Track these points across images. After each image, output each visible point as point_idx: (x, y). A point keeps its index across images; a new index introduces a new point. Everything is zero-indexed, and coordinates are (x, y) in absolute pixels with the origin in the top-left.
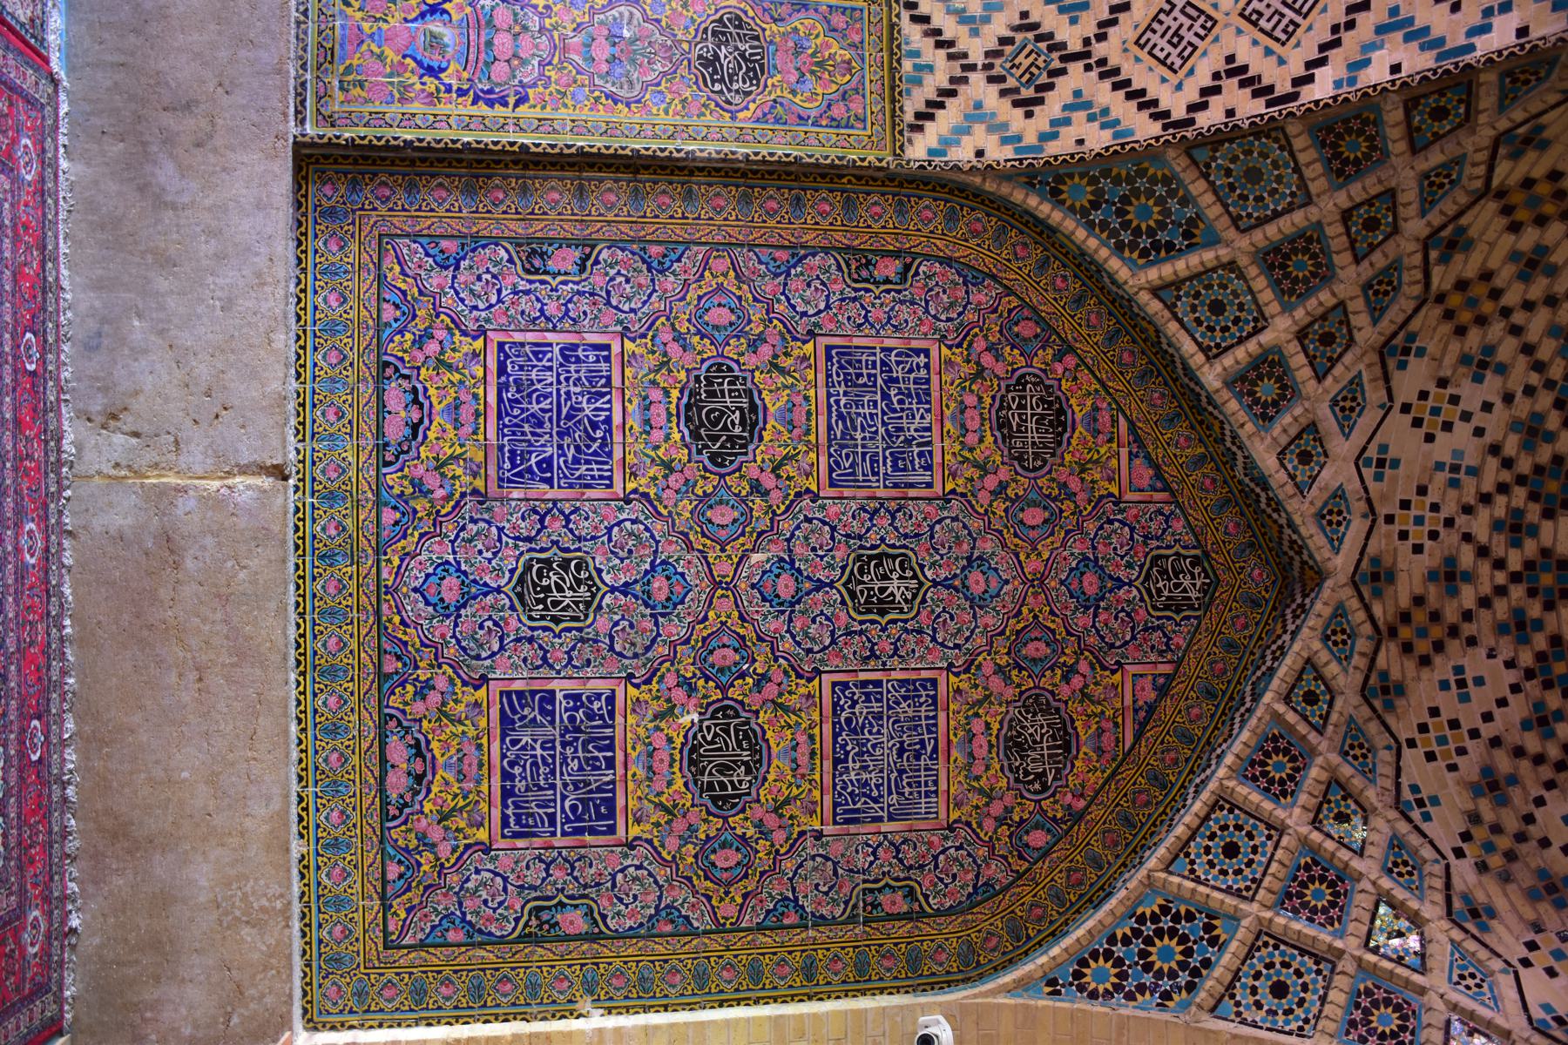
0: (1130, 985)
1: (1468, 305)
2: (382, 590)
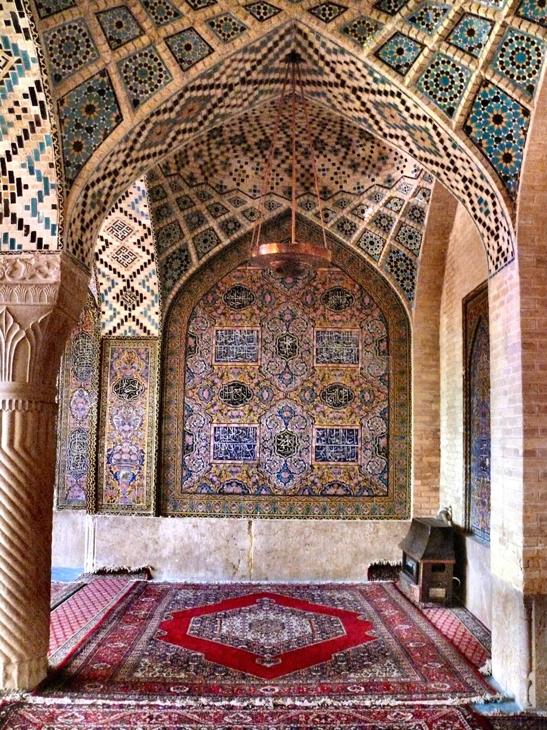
0: (410, 277)
1: (208, 170)
2: (285, 494)
